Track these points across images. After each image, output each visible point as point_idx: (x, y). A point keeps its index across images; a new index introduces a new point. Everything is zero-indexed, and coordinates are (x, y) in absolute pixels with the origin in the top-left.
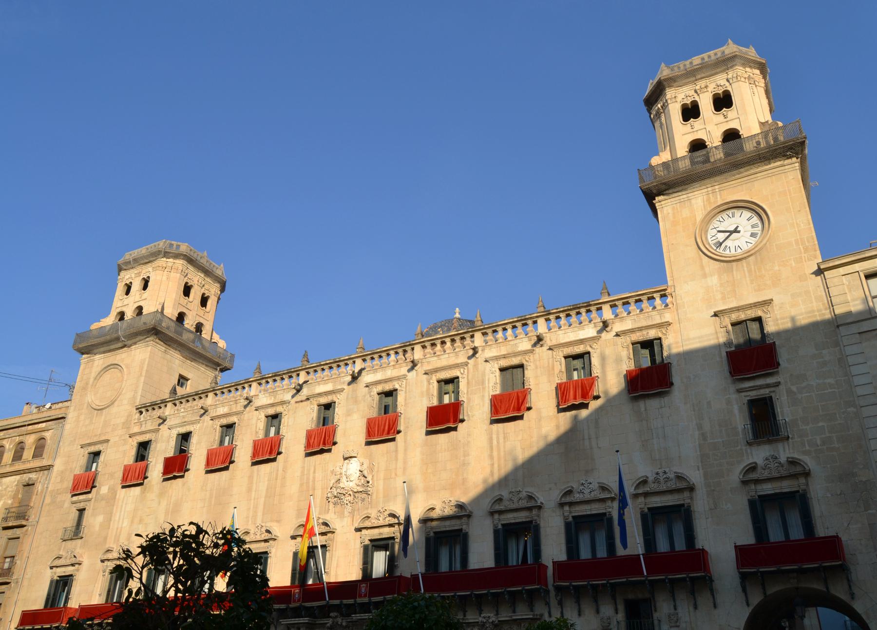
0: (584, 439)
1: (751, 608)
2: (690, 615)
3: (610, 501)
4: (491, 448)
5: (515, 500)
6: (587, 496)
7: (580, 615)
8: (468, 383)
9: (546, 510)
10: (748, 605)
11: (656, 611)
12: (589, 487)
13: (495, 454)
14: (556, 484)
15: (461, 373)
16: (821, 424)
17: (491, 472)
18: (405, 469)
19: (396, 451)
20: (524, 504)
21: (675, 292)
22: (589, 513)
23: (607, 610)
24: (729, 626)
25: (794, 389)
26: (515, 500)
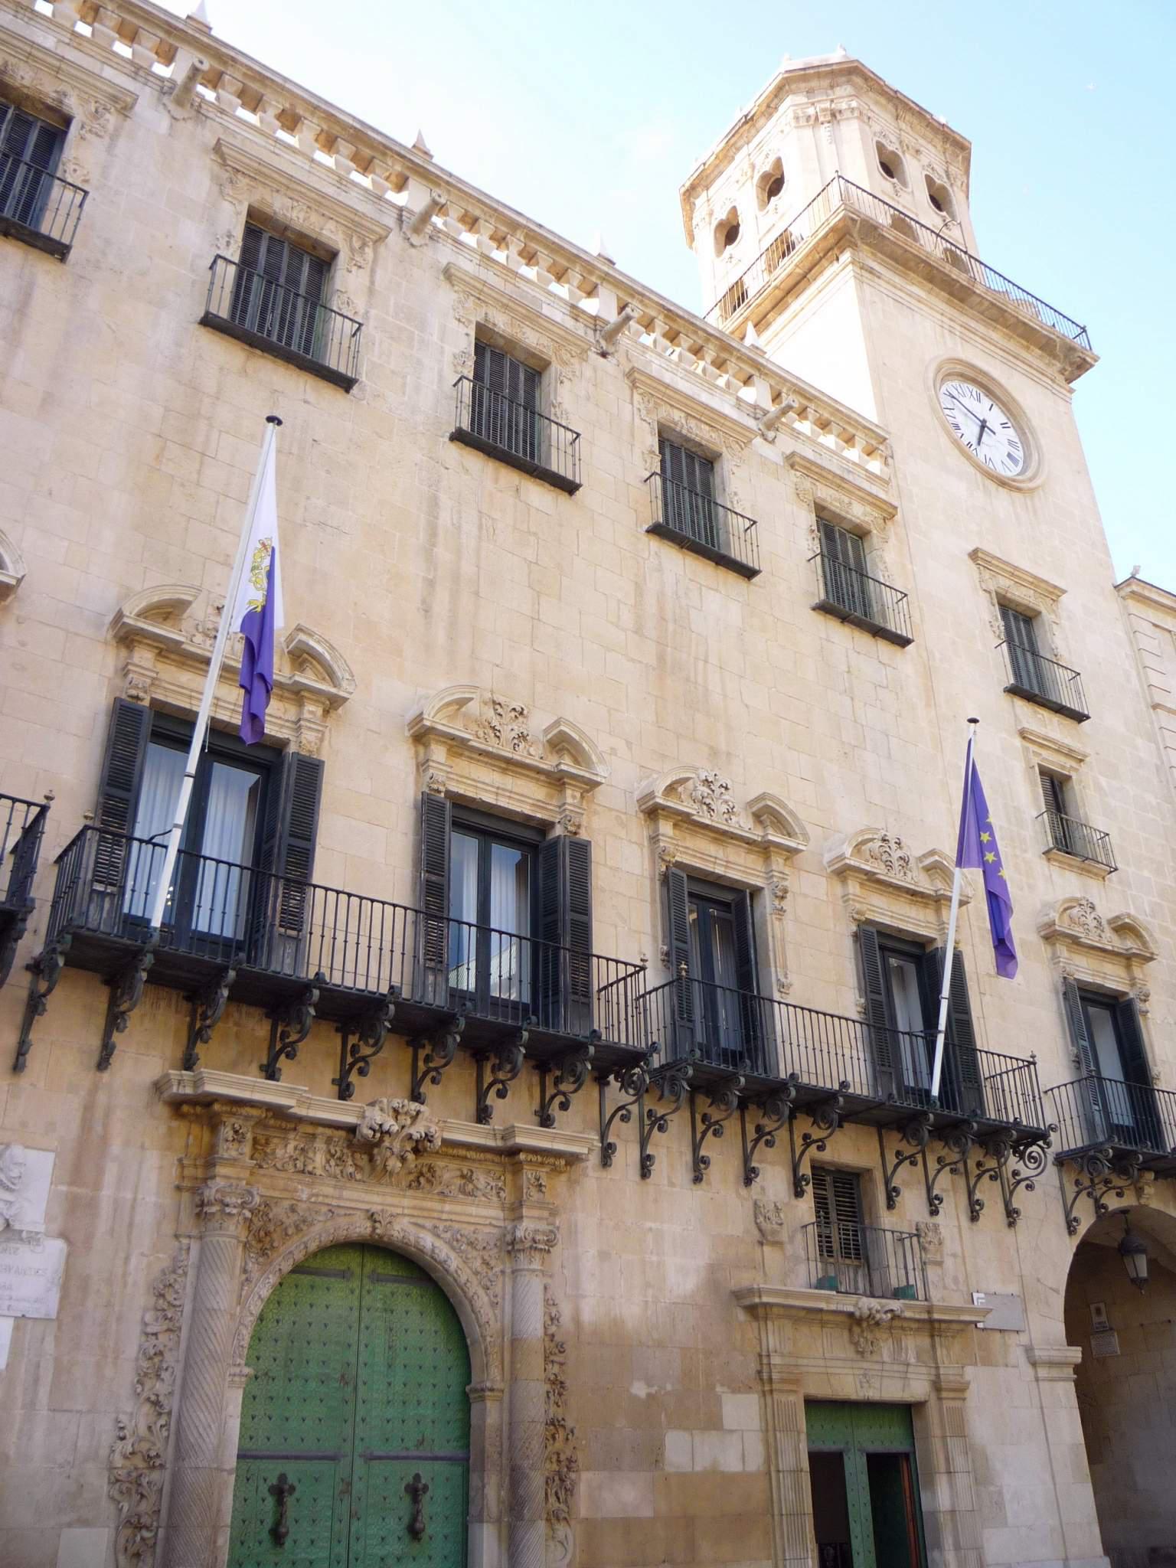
0: (706, 661)
1: (1076, 1240)
2: (961, 1236)
3: (781, 861)
4: (433, 533)
5: (507, 734)
6: (718, 822)
7: (697, 1179)
8: (371, 291)
9: (599, 808)
10: (1072, 1231)
11: (891, 1205)
12: (724, 797)
13: (443, 554)
14: (629, 744)
15: (352, 249)
16: (1146, 873)
17: (424, 602)
18: (48, 401)
19: (22, 308)
20: (534, 754)
21: (892, 457)
22: (719, 870)
23: (774, 1180)
24: (1038, 1280)
25: (1103, 781)
26: (507, 734)
